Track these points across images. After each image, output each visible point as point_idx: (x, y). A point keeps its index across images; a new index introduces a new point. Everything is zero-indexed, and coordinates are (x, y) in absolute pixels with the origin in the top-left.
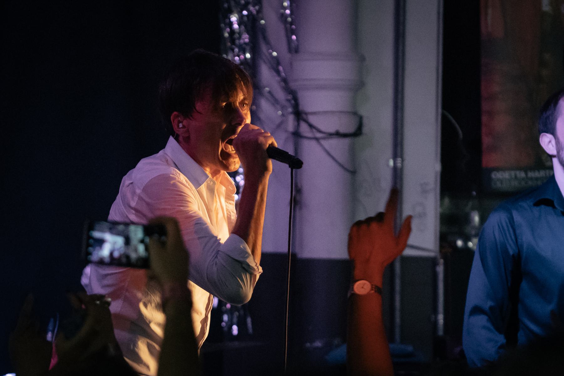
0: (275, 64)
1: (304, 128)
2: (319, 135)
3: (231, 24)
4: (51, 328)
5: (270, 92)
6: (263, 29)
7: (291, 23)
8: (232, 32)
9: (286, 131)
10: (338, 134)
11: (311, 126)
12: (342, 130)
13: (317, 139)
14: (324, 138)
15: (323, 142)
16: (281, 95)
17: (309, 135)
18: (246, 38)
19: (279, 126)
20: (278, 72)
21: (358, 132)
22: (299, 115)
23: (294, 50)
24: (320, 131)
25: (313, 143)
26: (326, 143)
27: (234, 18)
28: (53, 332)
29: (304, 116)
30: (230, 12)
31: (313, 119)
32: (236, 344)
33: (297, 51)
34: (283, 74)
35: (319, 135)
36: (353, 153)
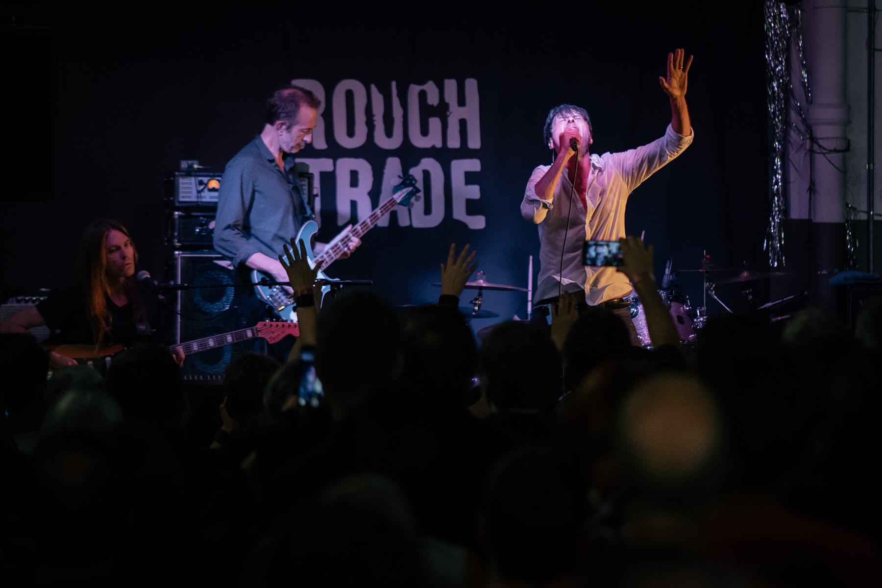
0: (799, 111)
1: (816, 147)
2: (824, 151)
3: (773, 88)
4: (668, 266)
5: (796, 126)
6: (792, 91)
7: (808, 87)
8: (774, 92)
9: (806, 149)
10: (835, 151)
11: (820, 146)
12: (838, 148)
13: (824, 154)
14: (827, 153)
15: (826, 155)
16: (802, 128)
17: (819, 151)
18: (782, 95)
19: (802, 145)
20: (801, 115)
21: (848, 148)
22: (813, 140)
23: (810, 102)
24: (825, 149)
25: (822, 155)
26: (829, 156)
27: (775, 85)
28: (669, 268)
29: (816, 140)
30: (773, 81)
31: (821, 142)
32: (777, 273)
33: (811, 103)
34: (804, 116)
35: (824, 151)
36: (844, 161)
